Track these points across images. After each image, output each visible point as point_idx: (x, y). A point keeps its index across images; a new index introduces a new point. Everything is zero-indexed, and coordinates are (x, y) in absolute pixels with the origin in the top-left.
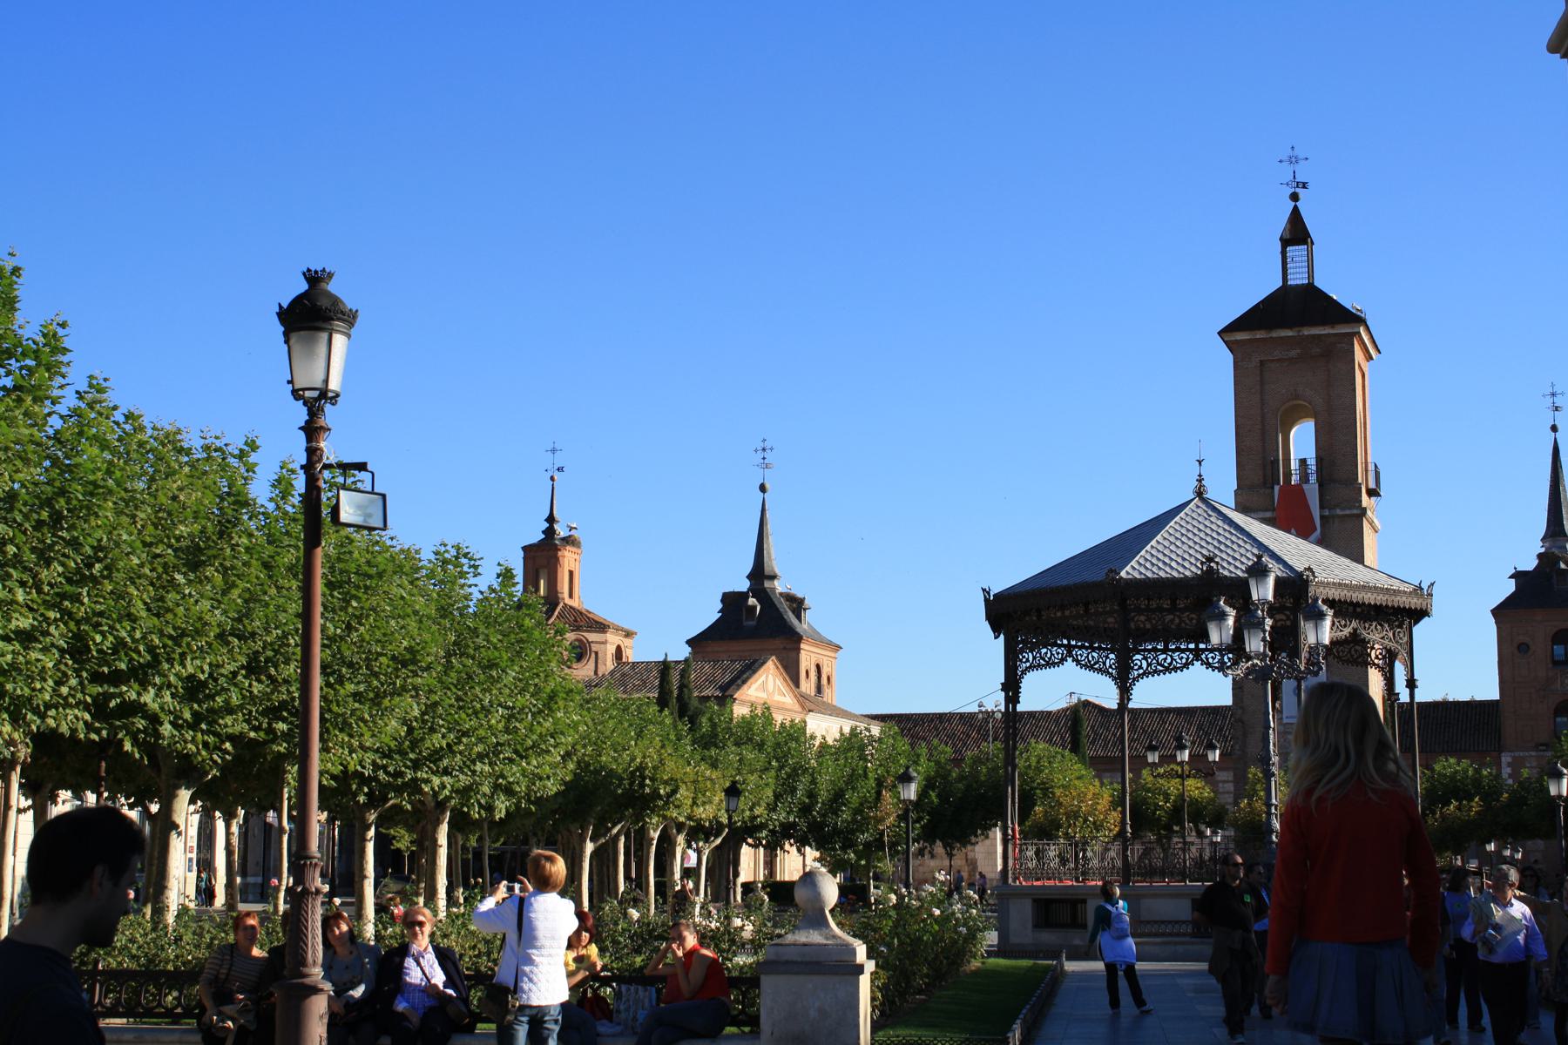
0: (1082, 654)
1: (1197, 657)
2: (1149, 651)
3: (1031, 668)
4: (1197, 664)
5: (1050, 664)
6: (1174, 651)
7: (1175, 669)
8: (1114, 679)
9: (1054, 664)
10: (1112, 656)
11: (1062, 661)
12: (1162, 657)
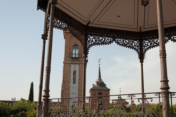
1: (114, 40)
4: (114, 42)
6: (105, 37)
7: (106, 44)
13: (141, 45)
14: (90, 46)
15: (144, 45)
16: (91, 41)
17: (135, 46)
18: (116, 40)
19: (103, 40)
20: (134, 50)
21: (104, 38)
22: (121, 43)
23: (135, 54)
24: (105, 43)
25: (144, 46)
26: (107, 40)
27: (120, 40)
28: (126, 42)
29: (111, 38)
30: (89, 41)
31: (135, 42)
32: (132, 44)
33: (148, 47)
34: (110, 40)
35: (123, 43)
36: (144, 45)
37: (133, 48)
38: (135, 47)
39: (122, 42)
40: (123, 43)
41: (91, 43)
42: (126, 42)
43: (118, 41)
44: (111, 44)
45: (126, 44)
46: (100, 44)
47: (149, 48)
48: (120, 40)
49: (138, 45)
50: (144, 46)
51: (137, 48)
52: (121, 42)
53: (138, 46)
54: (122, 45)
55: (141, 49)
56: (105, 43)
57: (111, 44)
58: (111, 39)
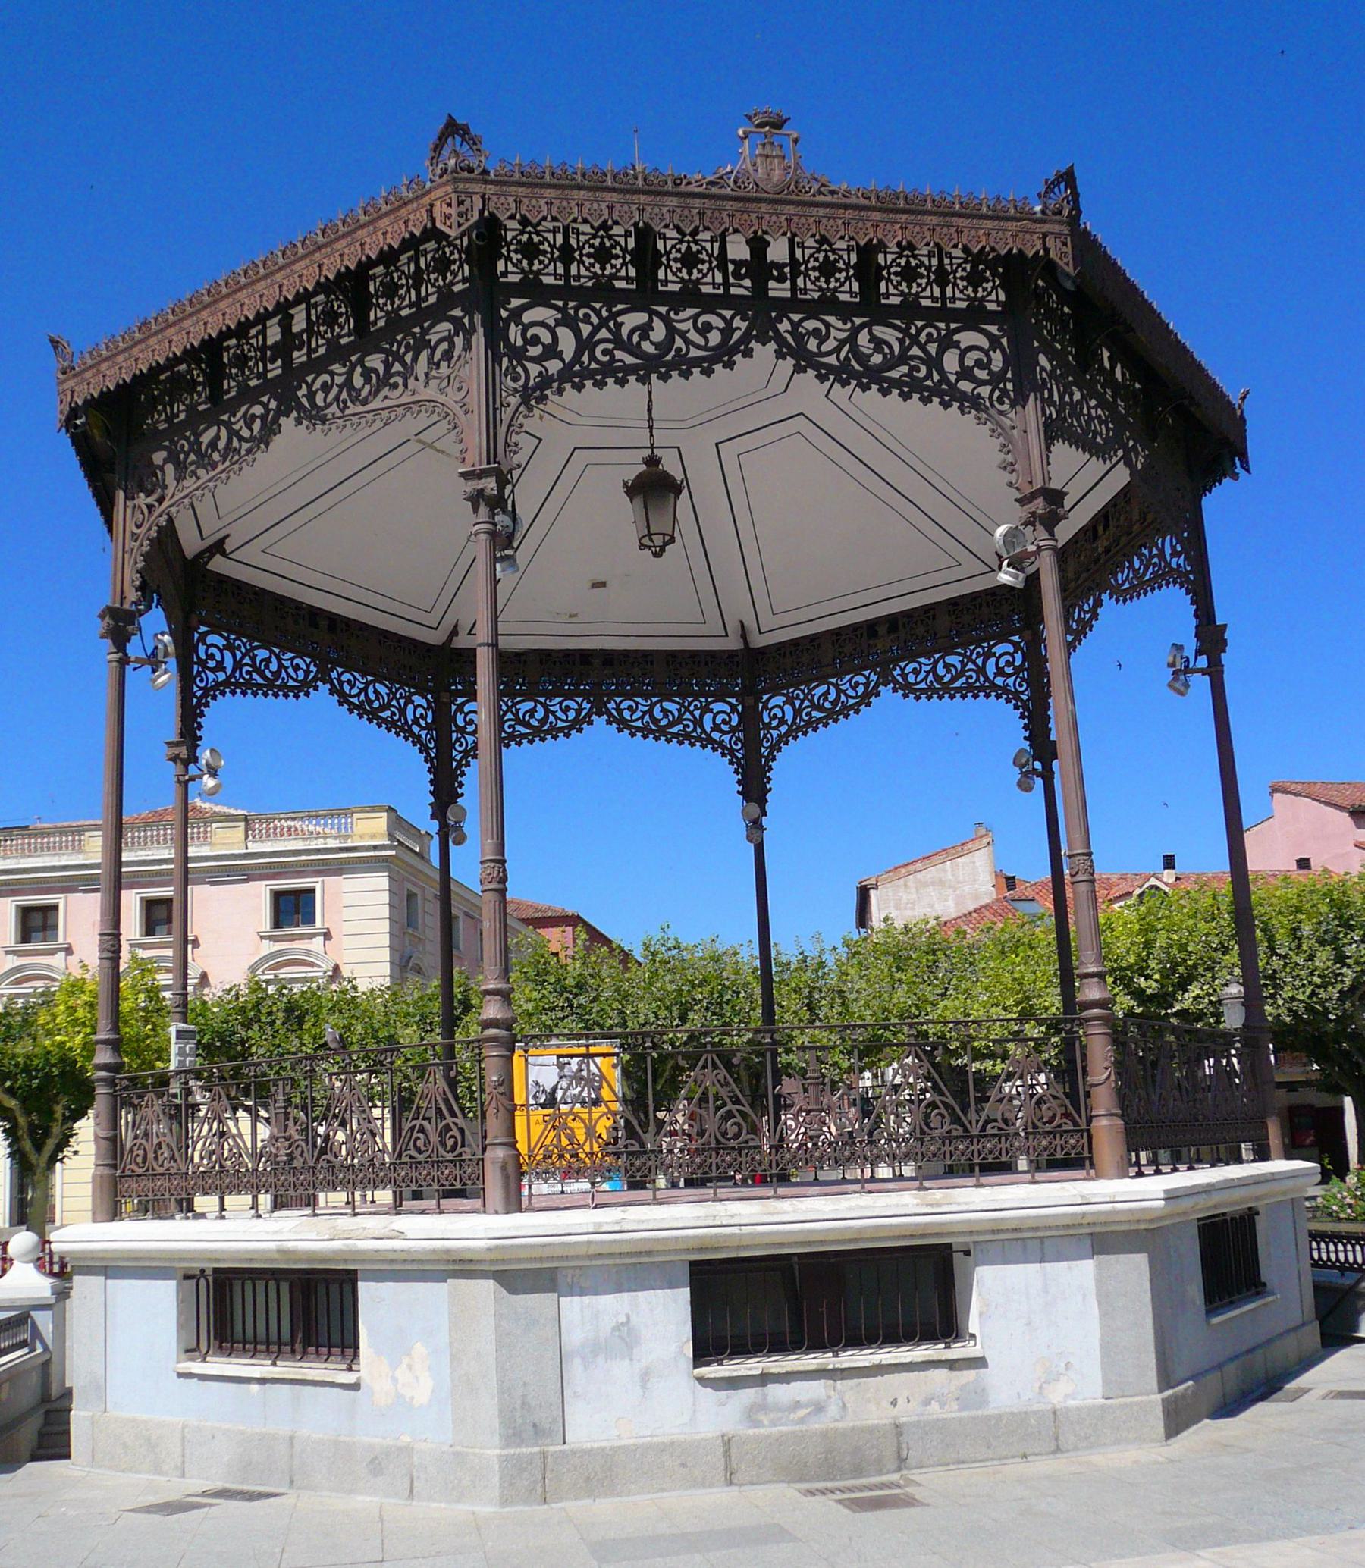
0: (353, 681)
1: (600, 709)
2: (585, 296)
4: (600, 721)
5: (274, 687)
6: (550, 696)
7: (554, 732)
8: (425, 749)
9: (285, 690)
10: (418, 700)
11: (304, 687)
12: (525, 706)
15: (766, 720)
17: (716, 728)
18: (784, 326)
19: (540, 713)
20: (714, 750)
23: (720, 775)
24: (547, 732)
25: (768, 727)
26: (693, 336)
27: (630, 708)
28: (664, 711)
29: (728, 314)
31: (717, 707)
32: (698, 723)
33: (784, 729)
36: (766, 720)
37: (707, 741)
38: (716, 735)
39: (837, 350)
42: (664, 711)
44: (730, 365)
45: (664, 722)
46: (523, 736)
48: (630, 708)
50: (768, 727)
52: (830, 345)
54: (646, 732)
55: (751, 744)
56: (547, 732)
57: (730, 365)
58: (729, 322)
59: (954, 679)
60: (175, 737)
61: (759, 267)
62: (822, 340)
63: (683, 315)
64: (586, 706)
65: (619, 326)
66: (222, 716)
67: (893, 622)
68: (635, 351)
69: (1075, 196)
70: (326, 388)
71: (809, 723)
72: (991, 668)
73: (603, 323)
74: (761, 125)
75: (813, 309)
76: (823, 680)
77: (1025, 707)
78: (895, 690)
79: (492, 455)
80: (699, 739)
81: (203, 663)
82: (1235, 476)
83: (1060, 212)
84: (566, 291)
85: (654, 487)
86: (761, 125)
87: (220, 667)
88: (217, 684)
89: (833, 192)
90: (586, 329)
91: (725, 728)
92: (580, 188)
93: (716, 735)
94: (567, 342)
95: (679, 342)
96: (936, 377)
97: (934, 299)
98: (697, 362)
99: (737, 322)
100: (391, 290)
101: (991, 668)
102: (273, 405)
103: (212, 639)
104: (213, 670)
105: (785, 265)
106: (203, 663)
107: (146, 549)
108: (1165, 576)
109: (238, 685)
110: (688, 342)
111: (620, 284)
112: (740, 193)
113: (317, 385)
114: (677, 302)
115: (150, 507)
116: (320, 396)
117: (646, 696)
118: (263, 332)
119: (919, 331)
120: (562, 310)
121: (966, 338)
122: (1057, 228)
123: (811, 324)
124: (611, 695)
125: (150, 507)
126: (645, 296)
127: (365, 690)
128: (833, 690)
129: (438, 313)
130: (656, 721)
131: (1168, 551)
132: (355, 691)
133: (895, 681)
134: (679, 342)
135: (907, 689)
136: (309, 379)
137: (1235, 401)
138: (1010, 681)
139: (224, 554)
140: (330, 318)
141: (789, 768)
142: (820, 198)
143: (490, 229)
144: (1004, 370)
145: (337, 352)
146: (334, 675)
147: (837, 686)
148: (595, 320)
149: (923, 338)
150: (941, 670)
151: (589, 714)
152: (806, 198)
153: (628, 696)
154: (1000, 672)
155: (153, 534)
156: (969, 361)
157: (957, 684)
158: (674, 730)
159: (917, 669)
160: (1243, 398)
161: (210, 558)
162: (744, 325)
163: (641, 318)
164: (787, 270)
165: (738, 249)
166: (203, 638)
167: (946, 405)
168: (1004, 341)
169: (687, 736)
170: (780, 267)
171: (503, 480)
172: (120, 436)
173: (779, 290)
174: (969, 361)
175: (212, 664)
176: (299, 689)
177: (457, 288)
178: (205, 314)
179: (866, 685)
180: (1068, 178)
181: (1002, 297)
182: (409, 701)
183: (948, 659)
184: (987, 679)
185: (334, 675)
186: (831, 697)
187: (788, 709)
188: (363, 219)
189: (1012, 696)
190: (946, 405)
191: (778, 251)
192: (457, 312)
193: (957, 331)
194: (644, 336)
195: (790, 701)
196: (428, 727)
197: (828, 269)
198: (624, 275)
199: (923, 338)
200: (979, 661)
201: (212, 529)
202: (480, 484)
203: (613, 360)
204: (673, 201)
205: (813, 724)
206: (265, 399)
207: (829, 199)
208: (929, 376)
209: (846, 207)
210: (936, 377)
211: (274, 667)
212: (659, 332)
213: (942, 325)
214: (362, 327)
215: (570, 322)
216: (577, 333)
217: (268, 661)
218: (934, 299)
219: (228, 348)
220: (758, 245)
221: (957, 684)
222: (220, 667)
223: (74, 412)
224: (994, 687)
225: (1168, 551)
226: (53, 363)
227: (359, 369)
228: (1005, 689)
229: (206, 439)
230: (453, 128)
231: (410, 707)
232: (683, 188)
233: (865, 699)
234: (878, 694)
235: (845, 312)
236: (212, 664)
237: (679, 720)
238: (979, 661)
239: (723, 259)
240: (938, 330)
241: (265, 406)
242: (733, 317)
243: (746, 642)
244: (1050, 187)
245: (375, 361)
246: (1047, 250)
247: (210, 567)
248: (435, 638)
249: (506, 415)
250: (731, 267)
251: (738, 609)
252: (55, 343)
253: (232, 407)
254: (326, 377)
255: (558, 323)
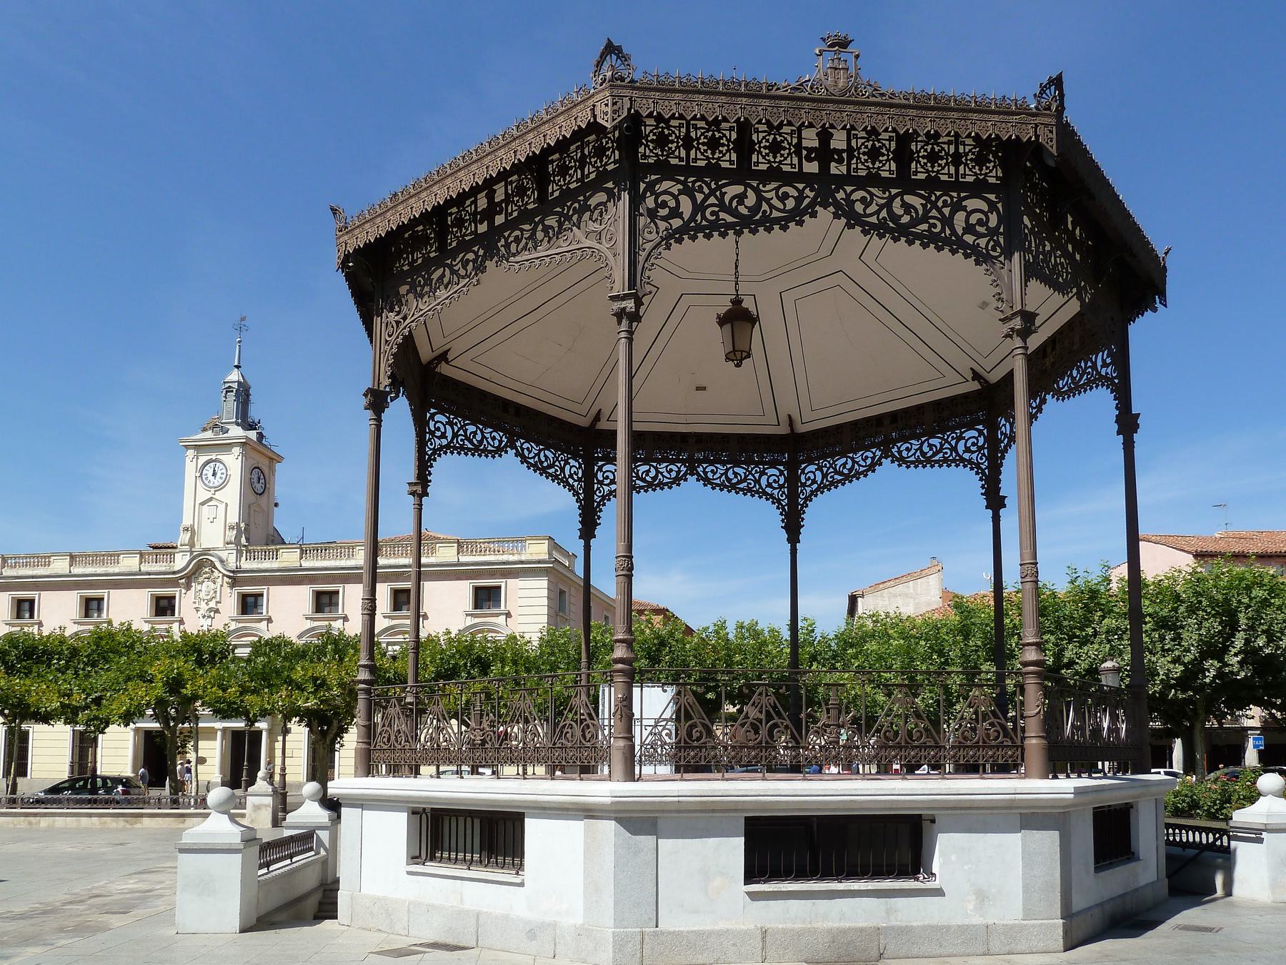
1: (692, 471)
2: (700, 173)
3: (449, 448)
4: (692, 479)
5: (478, 450)
6: (660, 461)
7: (661, 485)
8: (576, 494)
9: (486, 452)
10: (572, 462)
11: (499, 451)
13: (793, 482)
14: (603, 497)
16: (607, 482)
17: (769, 485)
18: (840, 195)
19: (653, 473)
21: (656, 468)
22: (874, 220)
23: (769, 516)
24: (658, 485)
25: (804, 485)
26: (775, 202)
28: (736, 474)
29: (801, 186)
30: (601, 483)
31: (770, 471)
32: (757, 481)
33: (815, 486)
34: (799, 199)
35: (884, 214)
38: (769, 490)
39: (878, 213)
40: (884, 214)
41: (606, 488)
42: (736, 474)
43: (705, 473)
44: (800, 223)
45: (735, 481)
47: (817, 490)
49: (782, 480)
50: (804, 485)
51: (776, 492)
53: (781, 487)
54: (722, 487)
55: (793, 497)
56: (658, 485)
57: (800, 223)
58: (801, 192)
59: (935, 454)
60: (413, 480)
61: (824, 154)
62: (867, 205)
63: (768, 187)
64: (684, 469)
65: (723, 194)
66: (443, 467)
67: (894, 417)
68: (734, 213)
69: (1062, 95)
70: (517, 240)
71: (832, 483)
72: (961, 447)
73: (712, 192)
74: (832, 46)
75: (861, 183)
76: (843, 455)
77: (983, 473)
78: (893, 462)
79: (632, 284)
80: (757, 492)
81: (432, 433)
82: (1155, 310)
83: (1049, 109)
84: (688, 170)
85: (738, 318)
86: (832, 46)
87: (443, 436)
88: (442, 447)
89: (882, 95)
90: (699, 197)
91: (775, 485)
92: (699, 92)
93: (769, 490)
94: (686, 206)
95: (765, 207)
96: (948, 232)
97: (950, 175)
98: (777, 221)
99: (807, 191)
100: (564, 171)
101: (961, 447)
102: (481, 252)
103: (438, 417)
104: (439, 438)
105: (843, 151)
106: (432, 433)
107: (394, 350)
108: (1097, 380)
109: (455, 448)
110: (772, 207)
111: (725, 165)
112: (816, 95)
113: (511, 239)
114: (765, 177)
115: (398, 323)
116: (513, 246)
117: (724, 463)
118: (475, 202)
119: (938, 198)
120: (684, 183)
121: (972, 204)
122: (1047, 120)
123: (861, 194)
124: (700, 462)
125: (398, 323)
126: (743, 173)
127: (538, 454)
128: (850, 461)
129: (596, 186)
130: (729, 480)
131: (1099, 363)
132: (532, 455)
133: (893, 456)
134: (765, 207)
135: (901, 461)
136: (506, 234)
137: (1161, 255)
138: (974, 456)
139: (447, 362)
140: (521, 191)
141: (816, 513)
142: (873, 99)
143: (635, 120)
144: (998, 226)
145: (526, 216)
146: (518, 444)
147: (852, 459)
148: (706, 190)
149: (940, 204)
150: (925, 449)
151: (685, 474)
152: (863, 99)
153: (711, 463)
154: (967, 450)
155: (400, 340)
156: (973, 220)
157: (936, 458)
158: (741, 486)
159: (909, 448)
160: (1166, 253)
161: (439, 363)
162: (812, 194)
163: (739, 189)
164: (845, 155)
165: (810, 139)
166: (433, 416)
167: (954, 252)
168: (1000, 206)
169: (750, 490)
170: (839, 152)
171: (639, 303)
172: (378, 273)
173: (835, 169)
174: (973, 220)
175: (438, 434)
176: (496, 452)
177: (610, 168)
178: (435, 188)
179: (873, 458)
180: (1057, 82)
181: (1000, 174)
182: (567, 463)
183: (932, 441)
184: (957, 454)
185: (518, 444)
186: (848, 466)
187: (818, 474)
188: (546, 118)
189: (976, 466)
190: (954, 252)
191: (839, 141)
192: (610, 185)
193: (966, 198)
194: (741, 202)
195: (820, 468)
196: (579, 480)
197: (874, 154)
198: (728, 160)
199: (940, 204)
200: (953, 443)
201: (439, 344)
202: (624, 304)
203: (718, 219)
204: (766, 102)
205: (834, 484)
206: (476, 249)
207: (879, 99)
208: (943, 230)
209: (891, 106)
210: (948, 232)
211: (479, 437)
212: (751, 199)
213: (955, 194)
214: (542, 198)
215: (688, 192)
216: (693, 199)
217: (475, 433)
218: (950, 175)
219: (451, 214)
220: (825, 136)
221: (936, 458)
222: (443, 436)
223: (347, 258)
224: (962, 460)
225: (1099, 363)
226: (333, 224)
227: (540, 227)
228: (970, 461)
229: (435, 276)
230: (611, 49)
231: (567, 467)
232: (773, 92)
233: (872, 468)
234: (881, 464)
235: (885, 184)
236: (438, 434)
237: (745, 480)
238: (953, 443)
239: (799, 146)
240: (952, 198)
241: (476, 253)
242: (804, 188)
243: (792, 429)
244: (1043, 89)
245: (552, 221)
246: (1037, 137)
247: (438, 370)
248: (584, 422)
249: (643, 255)
250: (804, 152)
251: (788, 406)
252: (334, 211)
253: (453, 254)
254: (517, 233)
255: (681, 192)
